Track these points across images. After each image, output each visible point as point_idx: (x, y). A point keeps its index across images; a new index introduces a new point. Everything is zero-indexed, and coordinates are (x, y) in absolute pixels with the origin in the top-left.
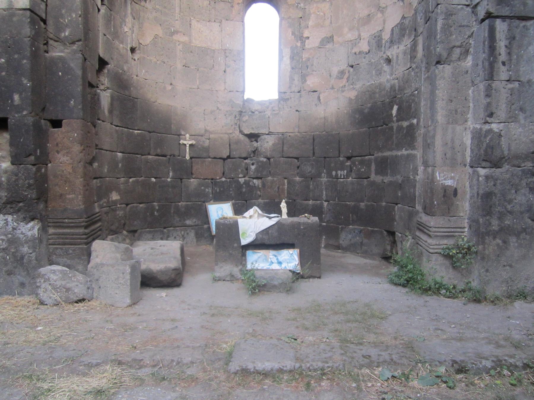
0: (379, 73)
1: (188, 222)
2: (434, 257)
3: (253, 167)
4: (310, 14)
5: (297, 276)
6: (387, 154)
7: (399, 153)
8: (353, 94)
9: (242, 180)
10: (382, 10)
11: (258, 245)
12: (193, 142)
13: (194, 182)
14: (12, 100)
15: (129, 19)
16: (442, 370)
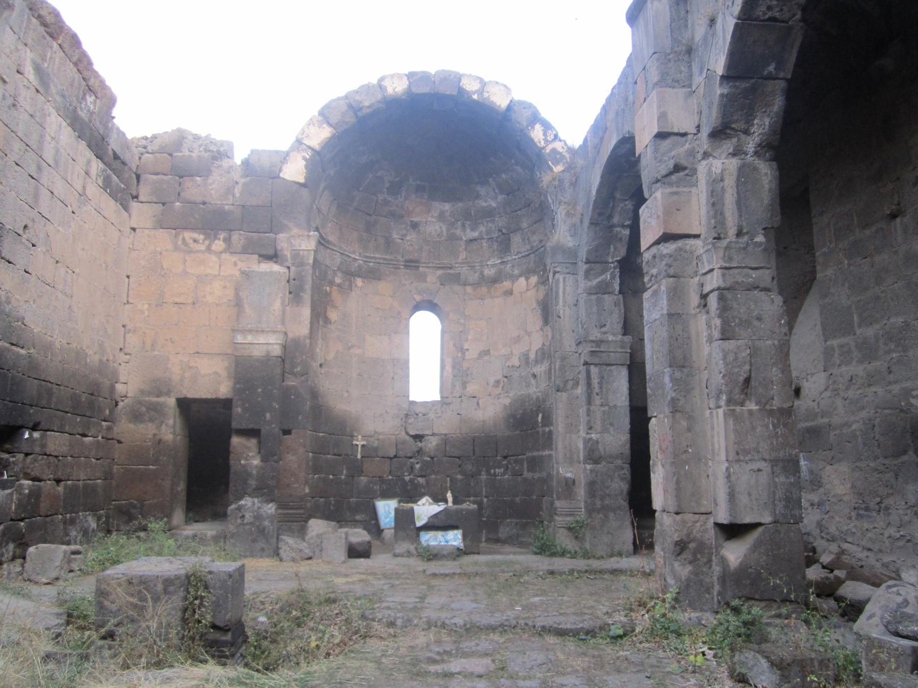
0: (528, 386)
1: (358, 517)
2: (561, 530)
3: (418, 466)
5: (459, 553)
6: (536, 454)
7: (544, 454)
8: (507, 401)
9: (407, 478)
10: (529, 334)
11: (430, 527)
12: (364, 443)
13: (363, 479)
14: (265, 417)
15: (320, 342)
16: (541, 573)
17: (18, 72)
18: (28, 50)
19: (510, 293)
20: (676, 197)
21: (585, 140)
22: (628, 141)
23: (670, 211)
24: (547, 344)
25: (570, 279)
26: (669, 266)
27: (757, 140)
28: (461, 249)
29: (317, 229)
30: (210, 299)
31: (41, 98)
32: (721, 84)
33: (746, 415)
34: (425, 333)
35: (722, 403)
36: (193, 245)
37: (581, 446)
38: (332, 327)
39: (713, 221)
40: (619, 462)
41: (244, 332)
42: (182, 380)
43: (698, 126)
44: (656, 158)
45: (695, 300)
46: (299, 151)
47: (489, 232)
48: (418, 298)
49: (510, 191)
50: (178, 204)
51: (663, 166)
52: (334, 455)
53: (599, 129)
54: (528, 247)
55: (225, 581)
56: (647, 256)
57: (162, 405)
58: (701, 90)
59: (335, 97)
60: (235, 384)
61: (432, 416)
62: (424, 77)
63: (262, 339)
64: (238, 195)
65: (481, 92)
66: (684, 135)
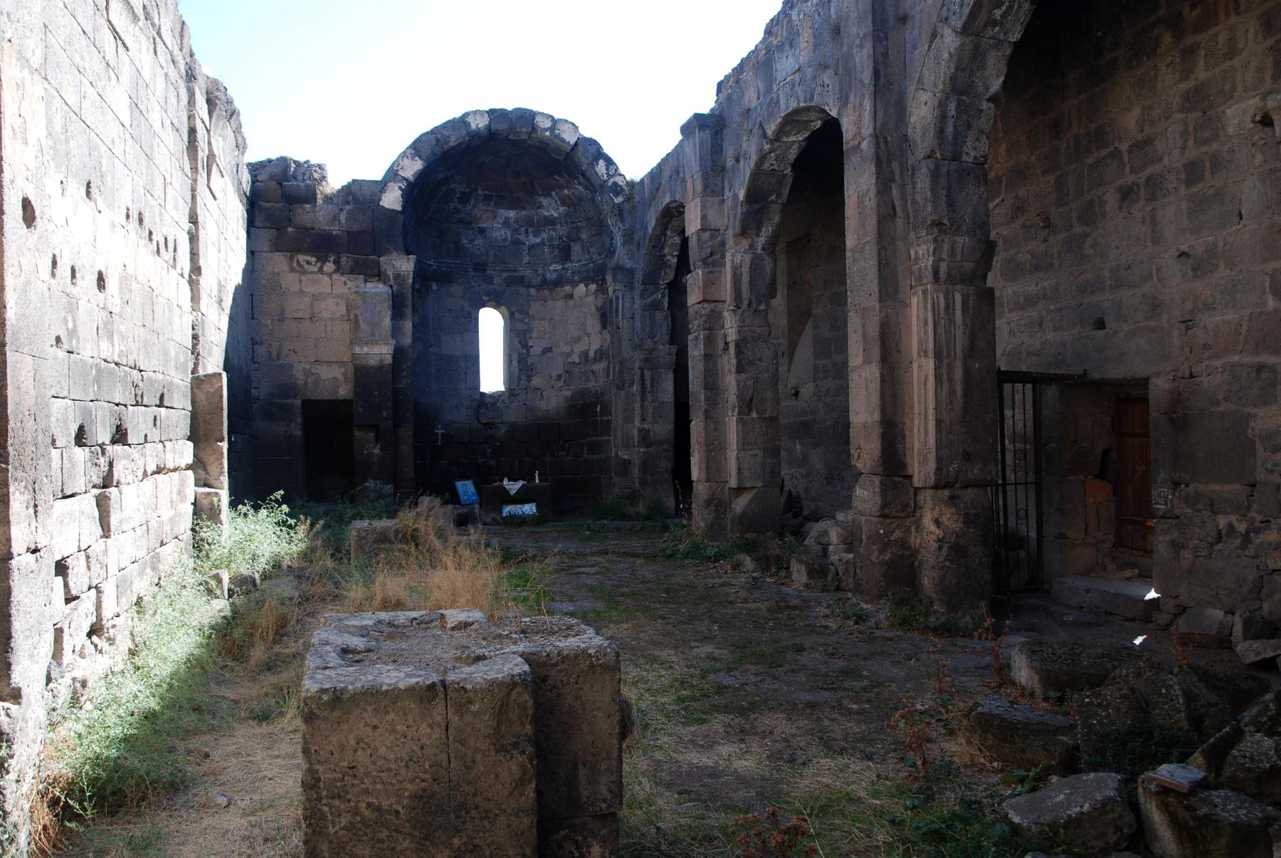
0: (588, 381)
8: (568, 393)
9: (480, 461)
19: (571, 296)
21: (642, 181)
30: (325, 315)
36: (306, 267)
40: (666, 446)
41: (362, 343)
42: (306, 383)
45: (721, 345)
47: (550, 239)
56: (691, 311)
60: (355, 388)
61: (500, 405)
63: (376, 350)
64: (343, 221)
65: (552, 129)
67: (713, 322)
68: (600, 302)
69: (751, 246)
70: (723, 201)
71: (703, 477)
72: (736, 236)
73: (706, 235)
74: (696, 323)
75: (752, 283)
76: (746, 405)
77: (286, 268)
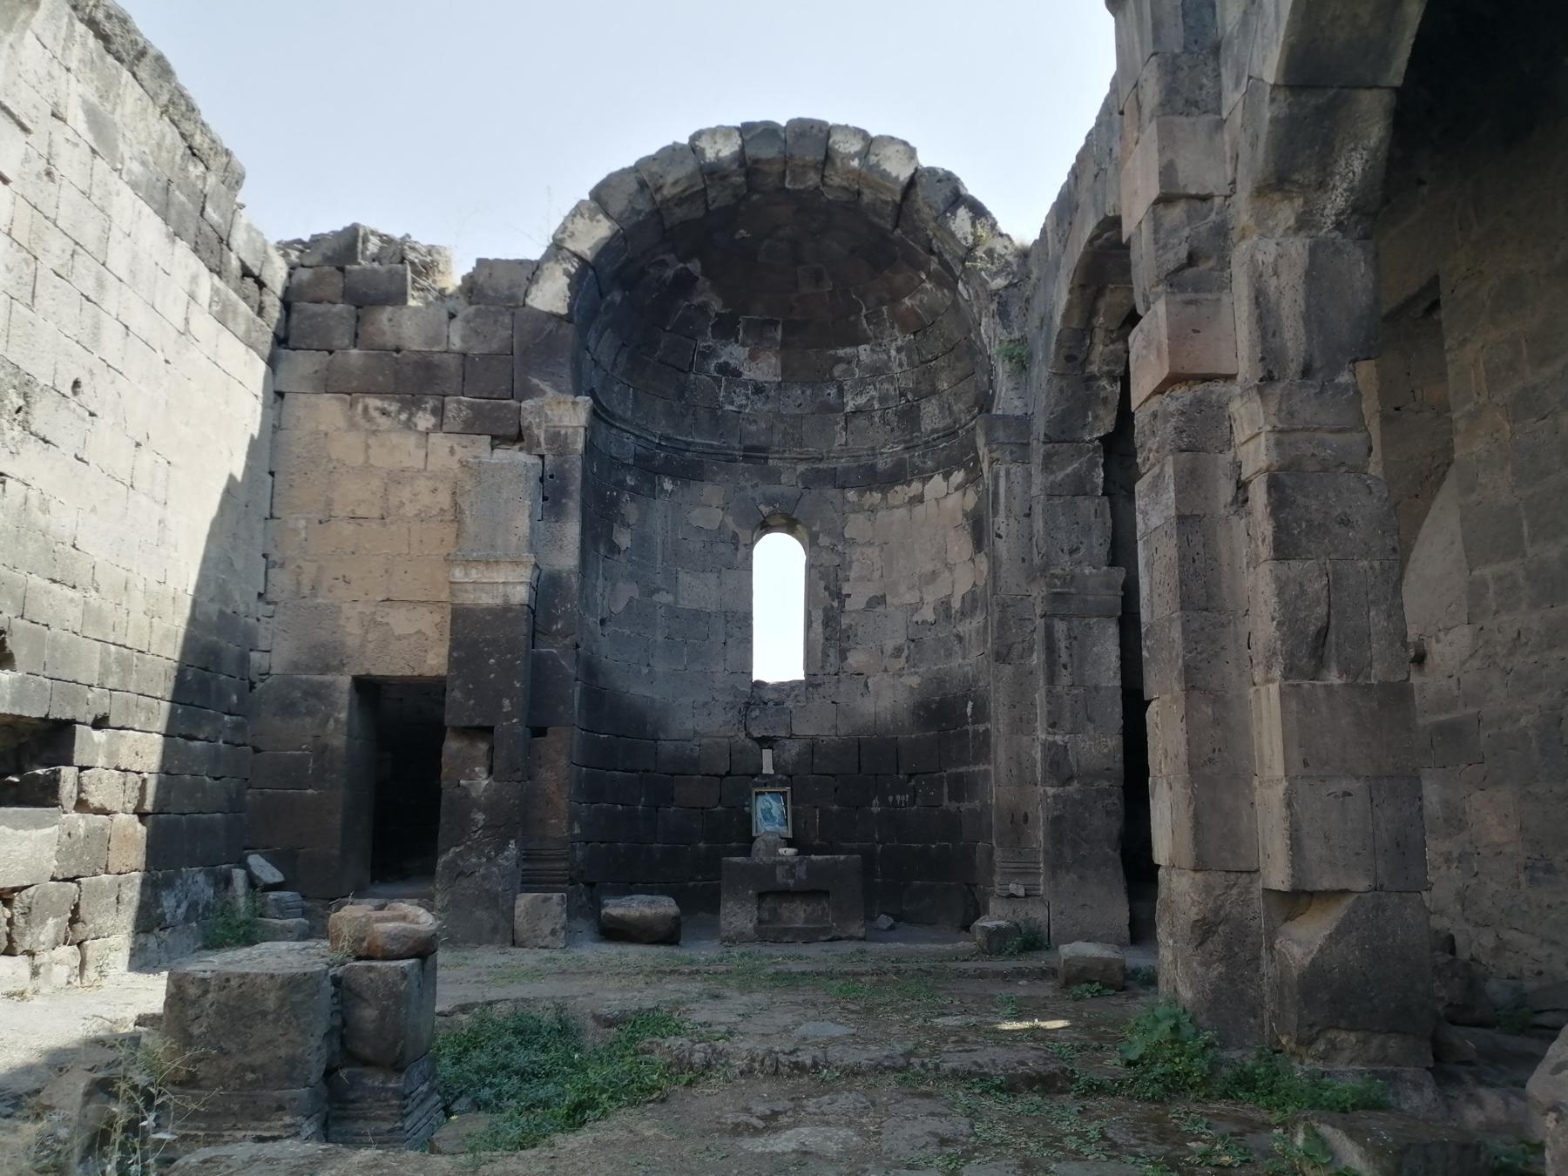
0: (949, 654)
4: (851, 562)
6: (962, 769)
8: (914, 681)
10: (950, 567)
15: (600, 582)
17: (53, 115)
18: (73, 80)
19: (920, 499)
20: (1192, 308)
21: (1044, 231)
22: (1112, 223)
23: (1180, 336)
24: (981, 583)
25: (1017, 469)
26: (1179, 431)
27: (1340, 202)
28: (837, 428)
29: (592, 393)
31: (101, 165)
32: (1273, 100)
33: (1321, 694)
34: (779, 568)
35: (1277, 673)
37: (1039, 756)
38: (622, 558)
39: (1258, 349)
41: (467, 563)
43: (1234, 182)
44: (1156, 241)
45: (1226, 491)
46: (557, 261)
48: (765, 509)
49: (919, 326)
50: (354, 352)
51: (1170, 255)
52: (626, 771)
53: (1065, 208)
54: (948, 421)
55: (395, 984)
56: (1141, 419)
57: (327, 686)
58: (1238, 118)
59: (616, 168)
60: (452, 649)
61: (789, 704)
62: (768, 131)
66: (1205, 198)
67: (1202, 433)
68: (971, 500)
69: (1304, 223)
70: (1220, 124)
71: (1187, 858)
72: (1260, 192)
73: (1177, 213)
74: (1153, 443)
75: (1314, 317)
76: (1310, 649)
77: (342, 423)
